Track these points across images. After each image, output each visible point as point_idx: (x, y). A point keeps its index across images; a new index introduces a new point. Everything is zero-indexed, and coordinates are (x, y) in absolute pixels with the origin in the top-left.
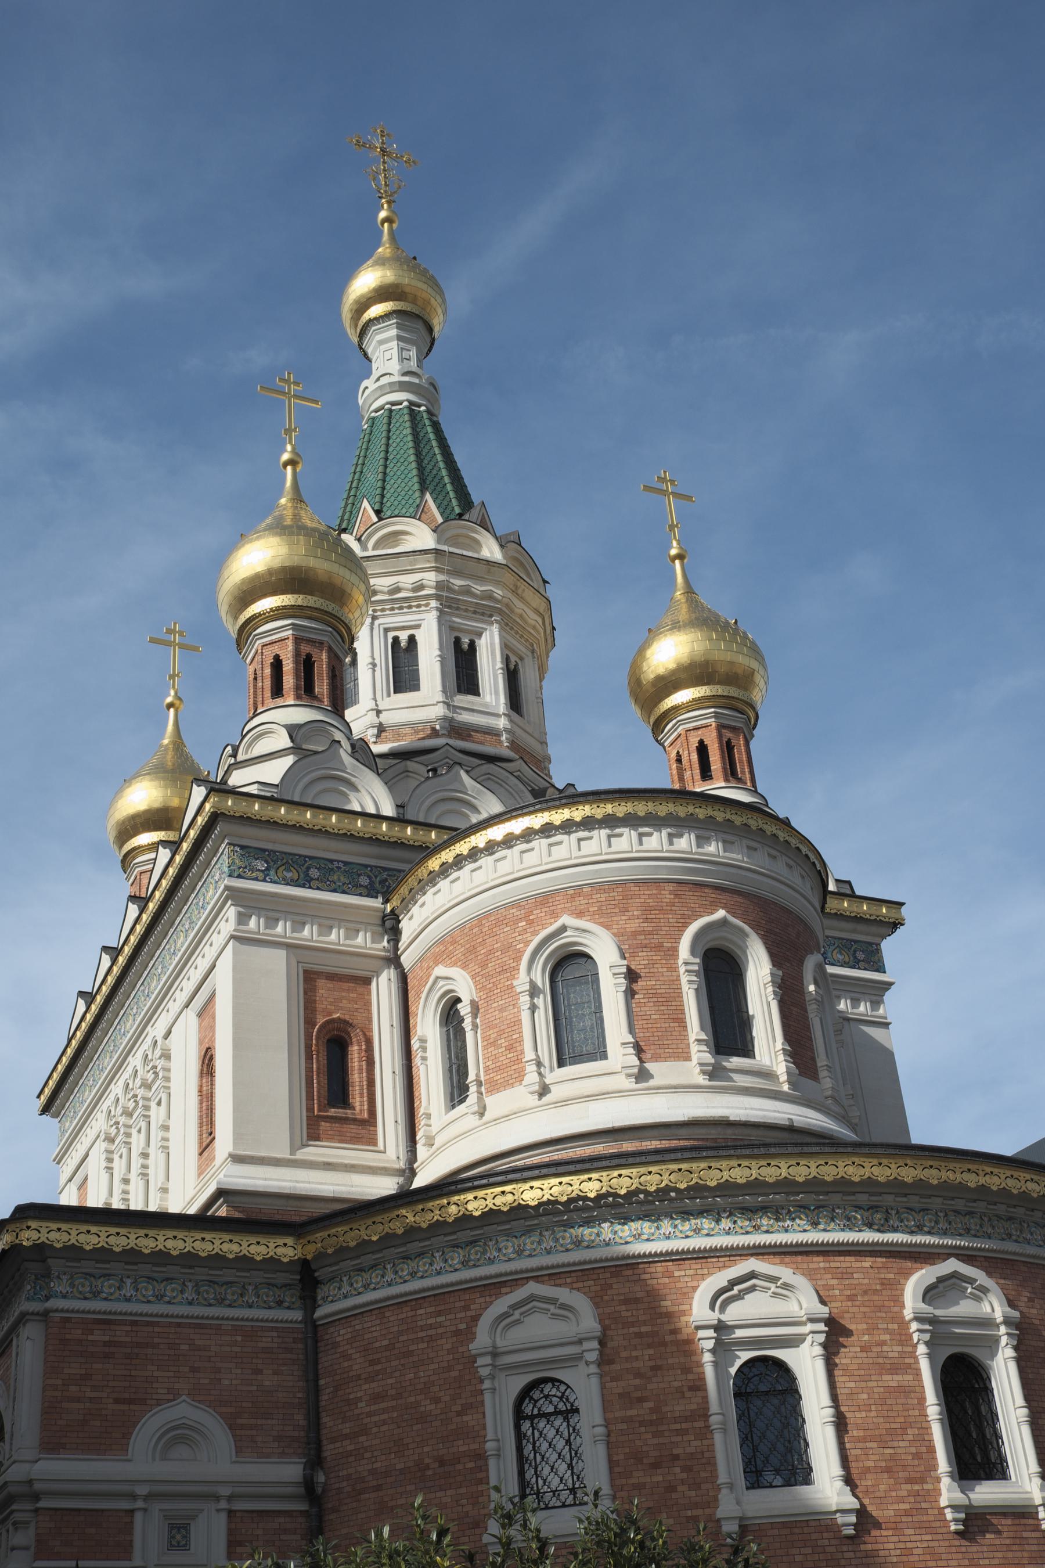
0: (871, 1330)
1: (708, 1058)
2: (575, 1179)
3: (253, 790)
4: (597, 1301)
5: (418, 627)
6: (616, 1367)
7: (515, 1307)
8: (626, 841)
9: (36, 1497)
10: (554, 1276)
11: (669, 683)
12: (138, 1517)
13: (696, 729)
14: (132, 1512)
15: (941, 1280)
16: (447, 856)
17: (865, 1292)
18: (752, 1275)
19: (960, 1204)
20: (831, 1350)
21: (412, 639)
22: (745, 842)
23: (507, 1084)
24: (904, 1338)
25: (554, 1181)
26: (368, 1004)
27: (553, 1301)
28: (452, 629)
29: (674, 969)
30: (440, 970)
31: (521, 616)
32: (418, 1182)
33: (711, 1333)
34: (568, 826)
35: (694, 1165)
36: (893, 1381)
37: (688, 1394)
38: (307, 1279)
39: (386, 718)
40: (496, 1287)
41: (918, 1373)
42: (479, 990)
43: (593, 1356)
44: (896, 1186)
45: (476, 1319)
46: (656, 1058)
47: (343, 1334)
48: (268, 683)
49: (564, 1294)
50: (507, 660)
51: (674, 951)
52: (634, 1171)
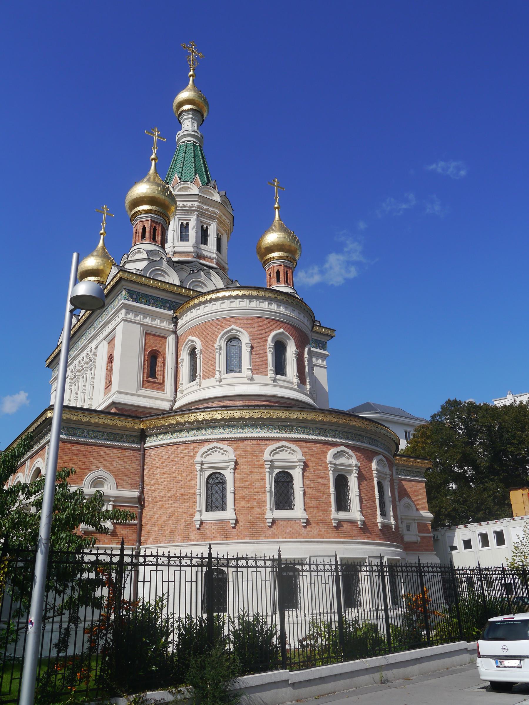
0: (317, 465)
1: (273, 375)
2: (232, 412)
3: (134, 271)
4: (235, 450)
5: (190, 220)
6: (239, 471)
7: (209, 450)
8: (255, 304)
11: (270, 249)
13: (277, 266)
15: (338, 452)
16: (197, 301)
17: (316, 454)
18: (283, 446)
19: (346, 430)
20: (304, 470)
21: (187, 224)
22: (292, 308)
23: (209, 377)
24: (326, 469)
25: (225, 412)
26: (165, 345)
27: (221, 449)
28: (201, 222)
29: (266, 346)
30: (190, 338)
31: (224, 221)
32: (177, 405)
33: (269, 463)
34: (236, 297)
35: (269, 411)
36: (321, 481)
37: (260, 481)
39: (176, 249)
41: (329, 479)
42: (203, 346)
43: (233, 467)
44: (329, 423)
46: (257, 374)
48: (140, 235)
49: (225, 447)
50: (218, 235)
51: (267, 340)
52: (251, 411)
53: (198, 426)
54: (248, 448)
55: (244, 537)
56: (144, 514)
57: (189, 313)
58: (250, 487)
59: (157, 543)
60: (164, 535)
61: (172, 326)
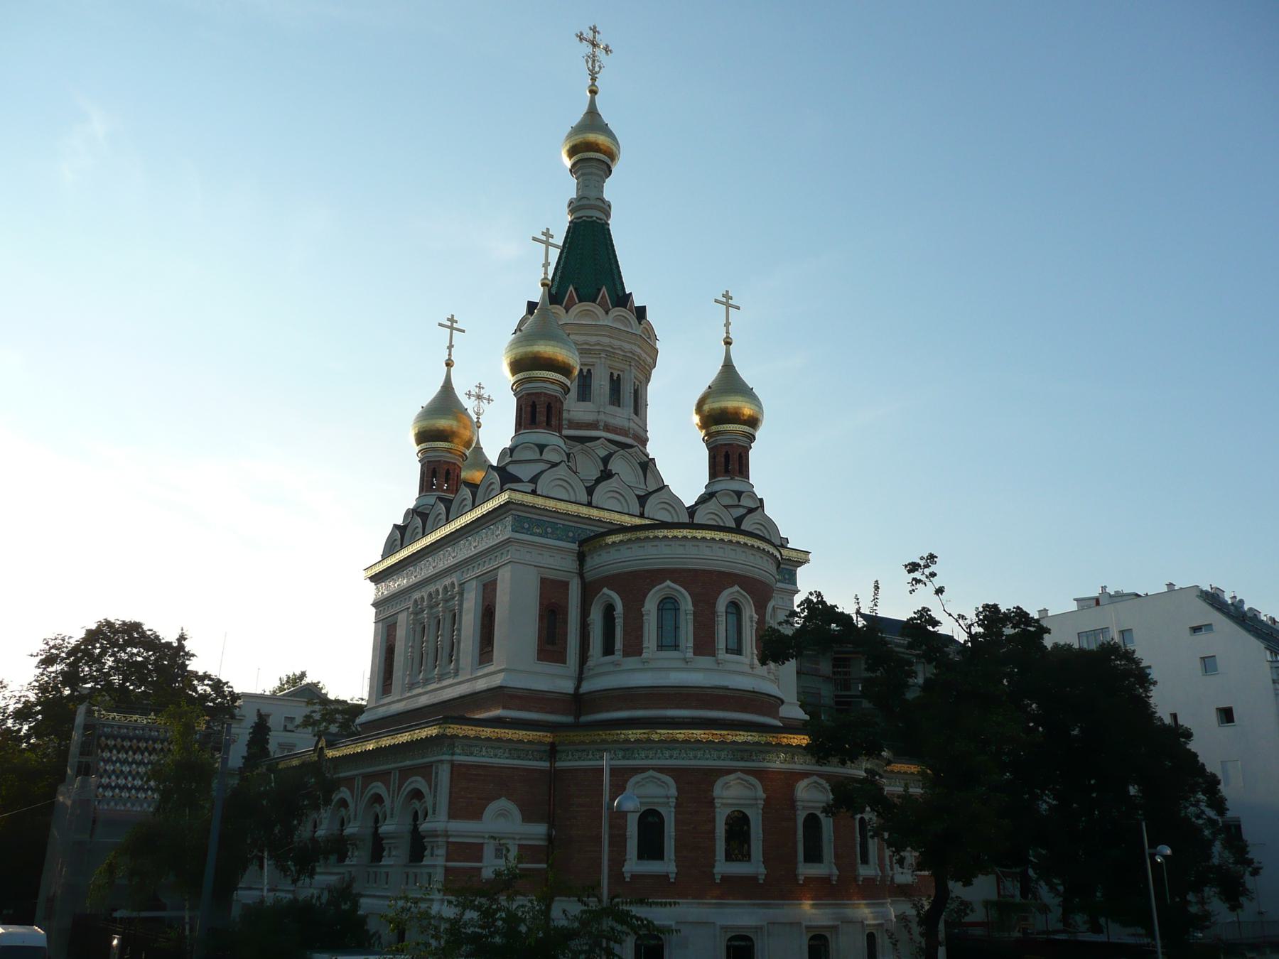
9: (448, 836)
10: (661, 770)
12: (485, 847)
14: (482, 844)
21: (589, 371)
30: (605, 590)
38: (553, 752)
45: (626, 781)
51: (714, 605)
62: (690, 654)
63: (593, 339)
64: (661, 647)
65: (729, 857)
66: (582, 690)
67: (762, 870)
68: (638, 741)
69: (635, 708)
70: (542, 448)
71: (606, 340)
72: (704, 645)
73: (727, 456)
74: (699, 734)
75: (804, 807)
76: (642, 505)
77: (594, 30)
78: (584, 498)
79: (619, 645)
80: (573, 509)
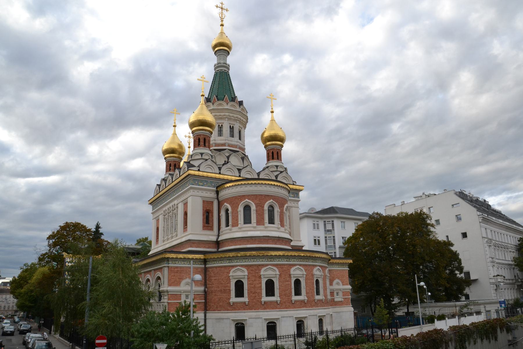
10: (242, 266)
29: (263, 210)
30: (225, 204)
38: (205, 261)
40: (233, 267)
47: (210, 270)
53: (230, 259)
54: (253, 269)
55: (252, 309)
56: (208, 298)
57: (224, 190)
58: (255, 287)
59: (214, 310)
60: (217, 308)
61: (216, 195)
62: (255, 225)
63: (222, 114)
64: (245, 223)
65: (267, 295)
66: (219, 240)
67: (279, 299)
68: (233, 257)
69: (236, 245)
70: (202, 154)
71: (227, 114)
72: (260, 222)
73: (273, 153)
74: (254, 253)
75: (294, 277)
76: (240, 173)
77: (222, 4)
78: (218, 171)
79: (230, 223)
80: (213, 175)
